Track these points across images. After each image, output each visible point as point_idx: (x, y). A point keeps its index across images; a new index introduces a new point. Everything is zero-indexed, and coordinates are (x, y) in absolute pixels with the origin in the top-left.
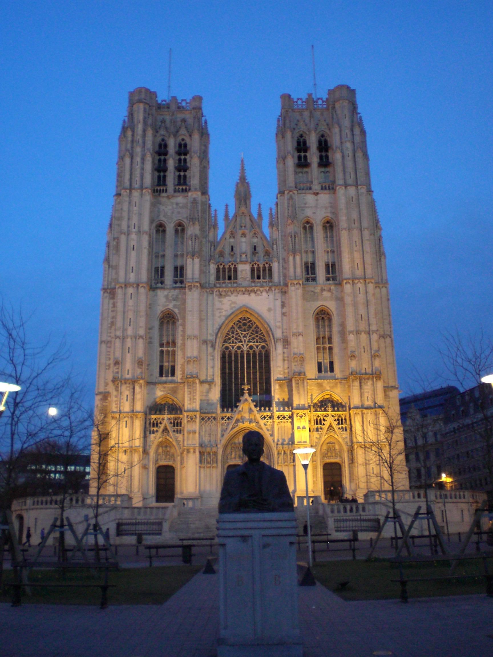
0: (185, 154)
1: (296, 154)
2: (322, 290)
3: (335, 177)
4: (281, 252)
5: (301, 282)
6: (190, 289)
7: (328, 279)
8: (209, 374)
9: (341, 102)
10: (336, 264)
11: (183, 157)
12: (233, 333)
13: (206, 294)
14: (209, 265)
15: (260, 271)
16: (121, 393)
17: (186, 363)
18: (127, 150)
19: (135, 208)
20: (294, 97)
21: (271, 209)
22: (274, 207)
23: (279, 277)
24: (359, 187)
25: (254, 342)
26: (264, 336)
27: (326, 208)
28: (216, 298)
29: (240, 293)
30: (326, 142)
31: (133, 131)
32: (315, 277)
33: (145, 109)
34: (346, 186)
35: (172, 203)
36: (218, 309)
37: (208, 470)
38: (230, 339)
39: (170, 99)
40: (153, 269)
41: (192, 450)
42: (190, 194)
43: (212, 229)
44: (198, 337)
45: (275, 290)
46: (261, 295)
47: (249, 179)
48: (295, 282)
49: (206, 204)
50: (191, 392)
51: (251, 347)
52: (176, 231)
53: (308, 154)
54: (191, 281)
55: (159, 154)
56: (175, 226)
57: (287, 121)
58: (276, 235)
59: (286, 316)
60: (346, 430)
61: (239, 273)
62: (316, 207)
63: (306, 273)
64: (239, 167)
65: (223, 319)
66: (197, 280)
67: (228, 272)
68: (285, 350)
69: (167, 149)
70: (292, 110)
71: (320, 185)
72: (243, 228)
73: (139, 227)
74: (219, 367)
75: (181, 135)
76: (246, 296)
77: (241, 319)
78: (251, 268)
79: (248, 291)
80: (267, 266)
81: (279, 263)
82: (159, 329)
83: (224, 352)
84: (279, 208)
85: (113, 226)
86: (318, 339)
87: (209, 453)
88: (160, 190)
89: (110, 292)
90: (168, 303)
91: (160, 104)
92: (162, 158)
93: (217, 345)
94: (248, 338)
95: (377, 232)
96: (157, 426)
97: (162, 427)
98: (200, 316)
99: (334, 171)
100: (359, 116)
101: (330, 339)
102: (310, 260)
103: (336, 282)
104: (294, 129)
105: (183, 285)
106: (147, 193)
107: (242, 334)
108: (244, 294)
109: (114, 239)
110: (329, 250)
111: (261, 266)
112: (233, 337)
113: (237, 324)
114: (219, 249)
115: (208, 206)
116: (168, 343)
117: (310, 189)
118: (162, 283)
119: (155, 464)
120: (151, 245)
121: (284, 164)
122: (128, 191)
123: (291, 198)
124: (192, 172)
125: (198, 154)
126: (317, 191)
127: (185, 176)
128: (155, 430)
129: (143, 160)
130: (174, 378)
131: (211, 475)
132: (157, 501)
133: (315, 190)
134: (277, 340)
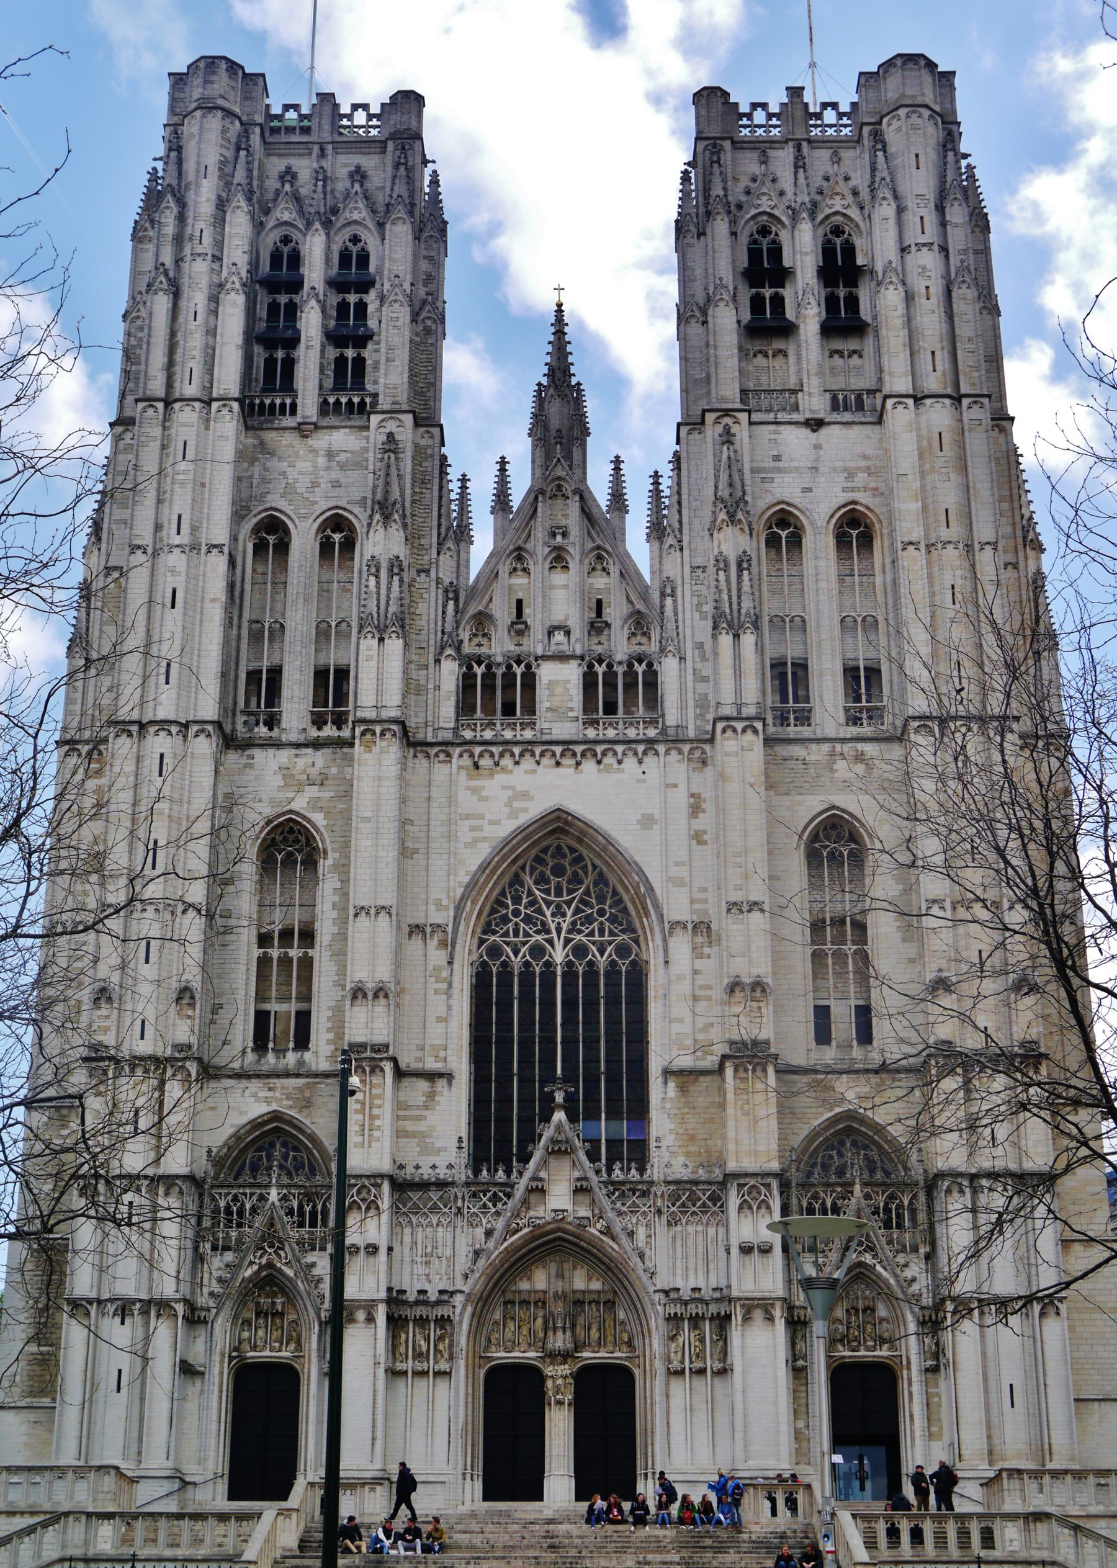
0: (365, 286)
1: (745, 295)
2: (832, 754)
3: (881, 371)
4: (688, 623)
5: (759, 725)
6: (368, 748)
7: (854, 720)
8: (429, 1042)
9: (902, 112)
10: (884, 668)
11: (352, 298)
12: (517, 900)
13: (424, 762)
14: (438, 661)
15: (615, 687)
17: (348, 1003)
18: (159, 266)
19: (183, 466)
20: (742, 98)
21: (656, 476)
22: (666, 471)
23: (683, 708)
24: (965, 402)
25: (591, 934)
26: (625, 910)
27: (850, 475)
29: (547, 761)
30: (849, 250)
31: (182, 204)
32: (810, 711)
33: (224, 131)
34: (918, 399)
35: (313, 451)
36: (468, 817)
37: (421, 1384)
38: (505, 920)
39: (315, 101)
40: (243, 676)
41: (361, 1315)
42: (375, 419)
43: (450, 544)
44: (394, 911)
45: (667, 752)
46: (619, 771)
47: (579, 373)
48: (739, 726)
49: (432, 456)
50: (363, 1104)
51: (580, 951)
52: (326, 548)
53: (787, 293)
54: (371, 714)
55: (272, 285)
56: (322, 528)
57: (717, 180)
58: (673, 567)
59: (705, 843)
60: (915, 1249)
61: (541, 693)
62: (815, 469)
63: (778, 698)
64: (549, 334)
65: (484, 851)
66: (394, 713)
67: (504, 688)
68: (699, 964)
69: (301, 270)
70: (733, 142)
71: (828, 395)
72: (559, 538)
73: (195, 529)
74: (466, 1019)
75: (349, 224)
77: (545, 850)
78: (585, 675)
79: (574, 755)
80: (640, 669)
81: (682, 659)
82: (260, 882)
83: (484, 964)
84: (684, 473)
85: (105, 526)
86: (817, 927)
87: (422, 1322)
88: (273, 405)
89: (90, 754)
90: (291, 795)
91: (279, 118)
92: (283, 299)
93: (459, 941)
94: (569, 918)
95: (1026, 557)
96: (240, 1225)
98: (402, 842)
99: (878, 350)
100: (964, 163)
101: (860, 928)
102: (792, 651)
103: (884, 728)
104: (739, 207)
105: (346, 733)
106: (225, 411)
107: (548, 904)
108: (558, 764)
109: (108, 570)
111: (620, 670)
112: (516, 913)
113: (533, 869)
114: (472, 610)
115: (437, 462)
116: (286, 935)
117: (796, 408)
118: (272, 722)
119: (231, 1358)
120: (234, 593)
121: (705, 323)
122: (160, 406)
123: (728, 438)
124: (383, 345)
125: (407, 286)
126: (821, 415)
127: (360, 362)
128: (234, 1234)
129: (214, 300)
130: (307, 1056)
131: (431, 1401)
132: (234, 1494)
133: (814, 412)
134: (675, 925)
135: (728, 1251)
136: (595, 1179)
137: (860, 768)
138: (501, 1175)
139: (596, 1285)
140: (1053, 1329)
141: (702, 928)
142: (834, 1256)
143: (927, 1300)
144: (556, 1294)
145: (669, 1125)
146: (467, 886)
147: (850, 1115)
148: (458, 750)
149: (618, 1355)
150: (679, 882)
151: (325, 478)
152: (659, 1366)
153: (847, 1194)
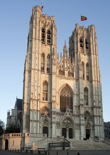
7: (87, 80)
16: (34, 103)
28: (59, 79)
37: (58, 129)
38: (62, 92)
41: (54, 123)
51: (68, 95)
53: (82, 44)
65: (61, 86)
68: (77, 98)
76: (67, 80)
83: (61, 96)
87: (58, 124)
97: (45, 115)
110: (87, 71)
118: (44, 72)
135: (80, 120)
136: (71, 114)
137: (88, 84)
138: (63, 113)
139: (70, 122)
140: (101, 127)
141: (77, 95)
142: (87, 121)
143: (92, 125)
144: (67, 123)
145: (75, 110)
146: (60, 89)
147: (87, 111)
148: (59, 77)
149: (71, 128)
150: (75, 91)
151: (48, 50)
152: (75, 128)
153: (87, 117)
